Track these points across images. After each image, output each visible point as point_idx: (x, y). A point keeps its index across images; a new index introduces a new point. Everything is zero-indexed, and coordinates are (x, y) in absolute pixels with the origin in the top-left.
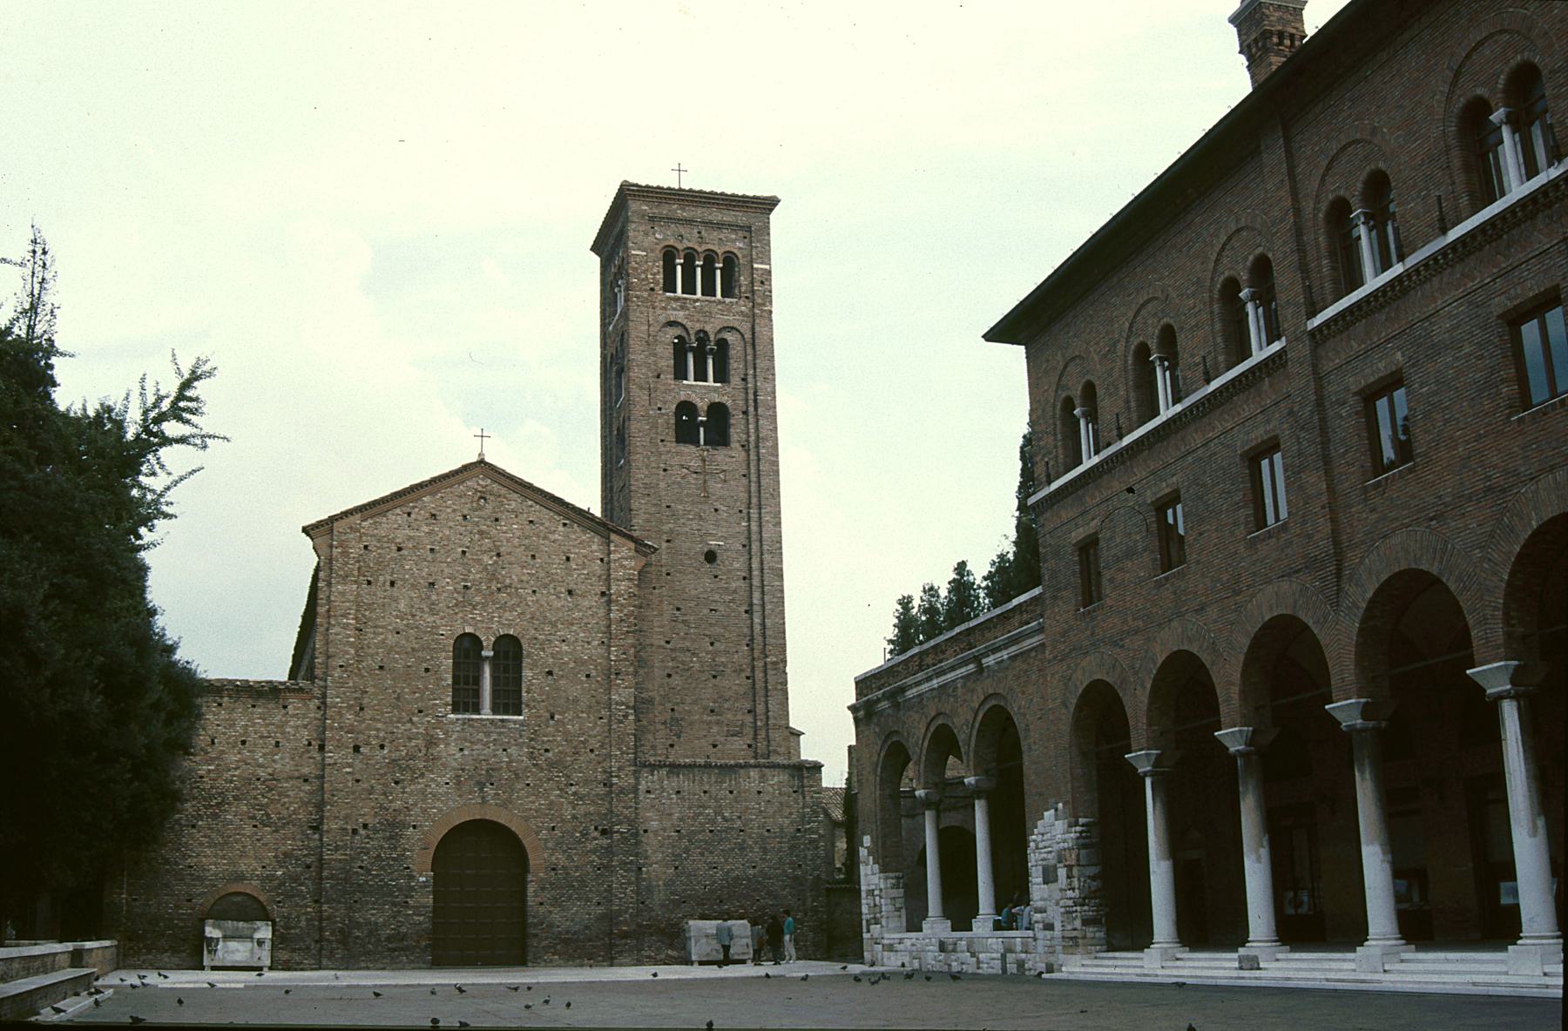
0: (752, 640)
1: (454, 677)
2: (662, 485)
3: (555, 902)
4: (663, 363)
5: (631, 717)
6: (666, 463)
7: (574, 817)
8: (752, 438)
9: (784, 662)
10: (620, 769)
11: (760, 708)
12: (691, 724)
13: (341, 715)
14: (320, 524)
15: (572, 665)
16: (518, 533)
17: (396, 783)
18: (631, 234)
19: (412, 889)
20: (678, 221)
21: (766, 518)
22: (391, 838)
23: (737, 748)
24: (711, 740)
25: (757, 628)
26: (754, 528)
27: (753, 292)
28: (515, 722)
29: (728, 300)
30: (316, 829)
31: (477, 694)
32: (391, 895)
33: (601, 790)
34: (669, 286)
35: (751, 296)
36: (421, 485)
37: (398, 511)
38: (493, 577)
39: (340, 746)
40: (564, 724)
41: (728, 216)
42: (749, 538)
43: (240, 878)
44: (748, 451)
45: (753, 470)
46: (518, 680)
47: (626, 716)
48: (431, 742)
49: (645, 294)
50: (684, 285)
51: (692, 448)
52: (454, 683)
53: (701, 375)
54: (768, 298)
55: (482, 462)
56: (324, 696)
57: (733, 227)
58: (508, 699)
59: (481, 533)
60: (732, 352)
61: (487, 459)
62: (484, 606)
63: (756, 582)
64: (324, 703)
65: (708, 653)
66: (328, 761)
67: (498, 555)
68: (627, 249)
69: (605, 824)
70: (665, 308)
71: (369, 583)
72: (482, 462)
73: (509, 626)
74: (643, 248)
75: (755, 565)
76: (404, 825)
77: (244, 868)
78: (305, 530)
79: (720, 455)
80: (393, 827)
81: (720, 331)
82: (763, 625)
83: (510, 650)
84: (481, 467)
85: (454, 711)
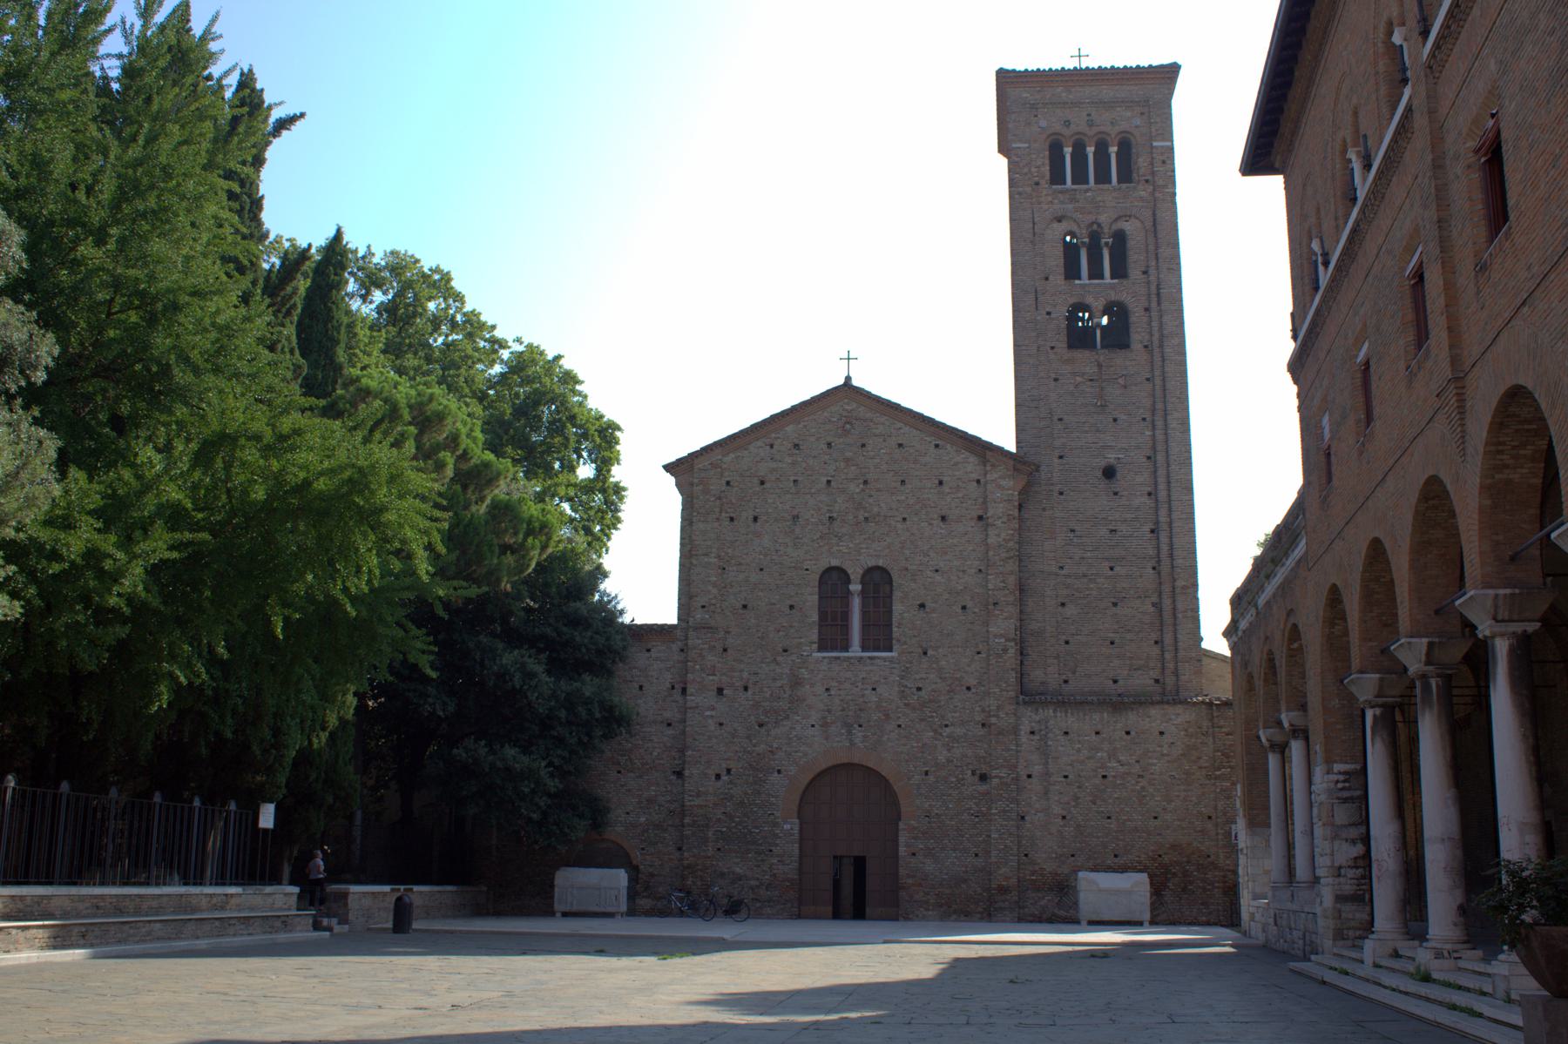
0: (1159, 562)
5: (1012, 651)
7: (949, 761)
9: (1195, 585)
10: (999, 708)
14: (680, 461)
15: (946, 596)
17: (761, 725)
21: (1173, 424)
25: (1165, 548)
27: (1153, 173)
28: (885, 659)
29: (1124, 186)
33: (982, 732)
37: (759, 443)
42: (1154, 448)
44: (1151, 353)
47: (1005, 650)
48: (796, 683)
49: (1028, 189)
51: (1087, 353)
53: (1096, 273)
58: (879, 635)
59: (847, 460)
60: (1131, 244)
61: (855, 383)
63: (1162, 494)
66: (689, 704)
69: (984, 769)
71: (732, 519)
79: (1119, 359)
81: (1116, 220)
83: (879, 582)
85: (820, 649)
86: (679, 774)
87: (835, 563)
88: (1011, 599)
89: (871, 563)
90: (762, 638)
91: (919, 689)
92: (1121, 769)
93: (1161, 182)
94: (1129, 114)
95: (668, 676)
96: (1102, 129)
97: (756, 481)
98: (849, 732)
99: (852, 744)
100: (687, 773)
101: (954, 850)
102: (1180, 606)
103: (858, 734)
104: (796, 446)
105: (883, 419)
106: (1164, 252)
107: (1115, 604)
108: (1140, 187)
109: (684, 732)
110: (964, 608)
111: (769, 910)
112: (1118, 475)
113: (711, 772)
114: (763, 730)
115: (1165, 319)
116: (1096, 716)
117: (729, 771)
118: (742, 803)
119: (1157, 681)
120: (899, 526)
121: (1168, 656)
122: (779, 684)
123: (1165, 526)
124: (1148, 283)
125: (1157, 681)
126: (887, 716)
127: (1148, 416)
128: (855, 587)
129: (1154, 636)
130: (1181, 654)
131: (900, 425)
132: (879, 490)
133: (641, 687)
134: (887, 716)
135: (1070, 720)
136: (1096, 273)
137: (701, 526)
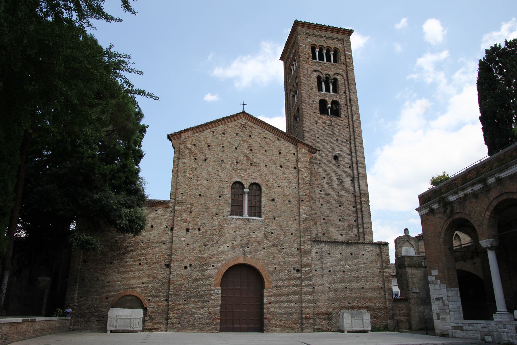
0: (355, 191)
1: (232, 200)
2: (316, 129)
6: (314, 123)
7: (285, 263)
8: (350, 114)
9: (368, 201)
11: (360, 220)
13: (181, 215)
14: (175, 134)
15: (283, 196)
16: (259, 142)
17: (205, 246)
18: (299, 38)
19: (211, 295)
20: (316, 36)
21: (357, 143)
22: (202, 271)
23: (351, 236)
25: (357, 187)
27: (346, 62)
28: (258, 220)
30: (168, 266)
31: (241, 206)
32: (201, 297)
34: (314, 57)
36: (219, 120)
37: (208, 131)
38: (248, 159)
39: (180, 228)
41: (336, 35)
43: (132, 288)
44: (348, 118)
45: (351, 126)
46: (260, 201)
47: (306, 219)
48: (221, 228)
50: (318, 60)
52: (232, 203)
53: (328, 90)
54: (352, 64)
55: (244, 112)
56: (174, 206)
57: (337, 39)
58: (256, 210)
59: (244, 141)
60: (339, 83)
63: (355, 168)
64: (174, 209)
65: (337, 196)
67: (251, 150)
68: (298, 44)
71: (196, 159)
72: (244, 112)
75: (354, 162)
76: (209, 266)
77: (133, 283)
78: (170, 137)
79: (337, 120)
80: (204, 264)
82: (359, 186)
85: (232, 215)
86: (168, 266)
87: (238, 180)
88: (308, 199)
89: (253, 181)
90: (207, 209)
91: (272, 233)
92: (350, 268)
95: (165, 222)
96: (328, 45)
97: (206, 145)
98: (244, 250)
99: (245, 255)
100: (172, 265)
101: (287, 301)
102: (364, 208)
103: (247, 251)
104: (223, 133)
106: (351, 87)
107: (340, 206)
109: (171, 247)
110: (289, 201)
111: (207, 329)
112: (340, 159)
113: (183, 265)
114: (206, 248)
115: (353, 108)
116: (340, 247)
117: (191, 265)
118: (196, 279)
119: (356, 235)
121: (360, 226)
122: (214, 228)
123: (356, 179)
124: (346, 96)
125: (356, 235)
126: (259, 244)
127: (349, 141)
128: (246, 190)
129: (355, 219)
130: (365, 225)
131: (264, 130)
132: (256, 153)
133: (152, 227)
134: (259, 244)
135: (331, 248)
136: (328, 90)
137: (183, 160)
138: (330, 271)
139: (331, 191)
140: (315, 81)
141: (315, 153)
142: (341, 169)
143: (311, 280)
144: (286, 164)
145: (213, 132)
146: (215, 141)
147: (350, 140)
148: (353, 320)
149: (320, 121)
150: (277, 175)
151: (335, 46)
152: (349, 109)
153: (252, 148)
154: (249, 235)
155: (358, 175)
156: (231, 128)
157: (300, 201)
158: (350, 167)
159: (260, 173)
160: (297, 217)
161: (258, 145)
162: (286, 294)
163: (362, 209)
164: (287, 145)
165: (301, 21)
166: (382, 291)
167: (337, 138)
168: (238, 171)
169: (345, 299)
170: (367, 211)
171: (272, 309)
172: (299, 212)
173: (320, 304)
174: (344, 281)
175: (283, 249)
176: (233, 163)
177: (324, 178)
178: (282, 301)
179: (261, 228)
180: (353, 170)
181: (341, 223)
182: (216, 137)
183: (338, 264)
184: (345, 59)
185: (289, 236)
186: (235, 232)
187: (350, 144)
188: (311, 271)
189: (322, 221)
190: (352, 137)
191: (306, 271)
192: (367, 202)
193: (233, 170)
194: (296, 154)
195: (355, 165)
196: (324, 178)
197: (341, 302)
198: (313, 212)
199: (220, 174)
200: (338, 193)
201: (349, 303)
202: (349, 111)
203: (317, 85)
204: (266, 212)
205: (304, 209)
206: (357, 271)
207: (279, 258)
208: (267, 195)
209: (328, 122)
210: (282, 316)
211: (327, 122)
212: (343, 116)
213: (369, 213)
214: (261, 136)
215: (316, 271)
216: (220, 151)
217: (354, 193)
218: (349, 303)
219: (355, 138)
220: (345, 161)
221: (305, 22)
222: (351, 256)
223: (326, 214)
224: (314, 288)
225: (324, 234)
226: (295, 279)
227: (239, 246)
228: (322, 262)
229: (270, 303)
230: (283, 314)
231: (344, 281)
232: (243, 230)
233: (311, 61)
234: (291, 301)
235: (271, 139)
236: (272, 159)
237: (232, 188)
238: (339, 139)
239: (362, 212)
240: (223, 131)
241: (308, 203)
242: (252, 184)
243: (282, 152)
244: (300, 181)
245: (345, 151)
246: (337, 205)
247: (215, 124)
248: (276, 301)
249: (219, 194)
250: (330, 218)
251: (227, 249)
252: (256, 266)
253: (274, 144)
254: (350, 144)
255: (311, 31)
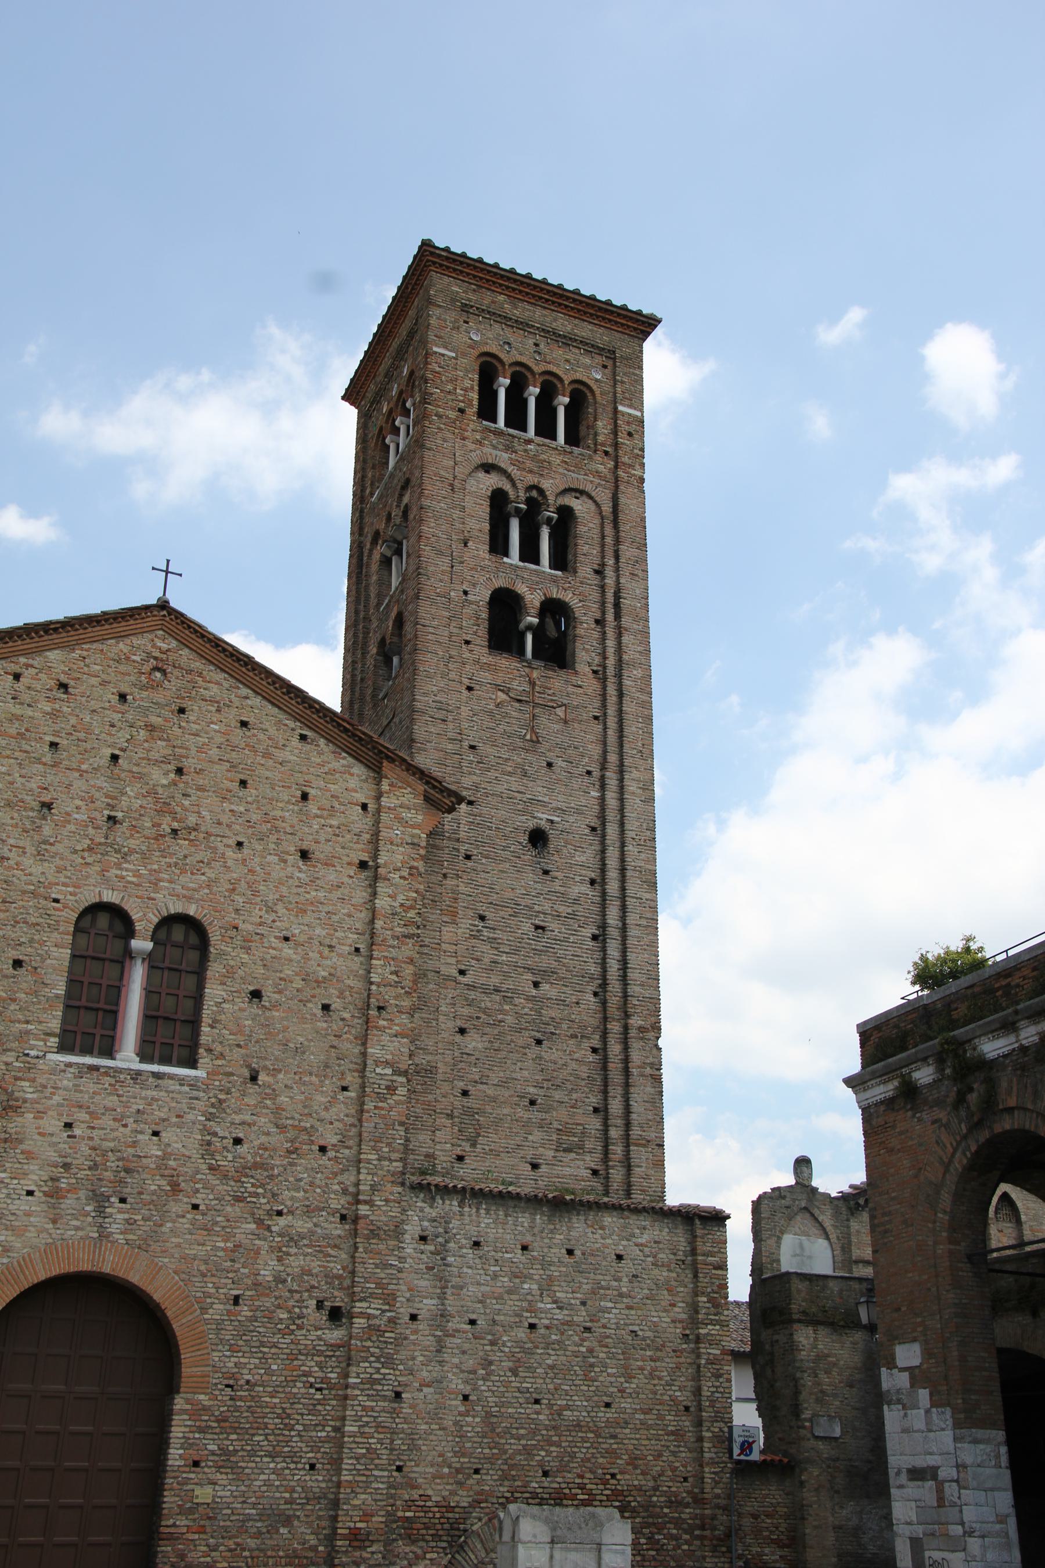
0: (604, 984)
1: (73, 982)
2: (465, 712)
3: (226, 1460)
4: (472, 524)
5: (402, 1091)
7: (279, 1280)
8: (611, 662)
9: (657, 1028)
10: (374, 1188)
11: (616, 1106)
12: (498, 1121)
15: (298, 984)
16: (219, 739)
18: (433, 321)
20: (505, 320)
21: (631, 786)
23: (573, 1172)
24: (529, 1154)
25: (614, 966)
26: (612, 801)
27: (616, 445)
28: (181, 1081)
31: (112, 1015)
33: (339, 1230)
34: (487, 411)
35: (614, 453)
36: (47, 628)
38: (164, 808)
40: (274, 1095)
41: (585, 330)
44: (604, 681)
45: (611, 711)
46: (198, 998)
47: (391, 1089)
52: (69, 994)
53: (530, 554)
54: (639, 455)
55: (163, 605)
57: (591, 348)
58: (174, 1036)
59: (151, 728)
60: (581, 529)
62: (145, 857)
63: (613, 887)
65: (530, 999)
67: (180, 771)
68: (424, 342)
69: (339, 1299)
70: (480, 443)
72: (163, 605)
73: (189, 899)
74: (454, 347)
75: (612, 862)
79: (557, 682)
82: (624, 962)
84: (163, 614)
85: (64, 1048)
87: (109, 896)
88: (406, 1003)
91: (238, 1141)
92: (560, 1315)
93: (625, 459)
94: (588, 361)
96: (555, 370)
98: (100, 1211)
99: (104, 1236)
101: (273, 1456)
102: (636, 1056)
104: (63, 686)
105: (220, 676)
106: (627, 552)
107: (539, 1042)
108: (598, 457)
110: (326, 1008)
115: (625, 639)
116: (524, 1219)
119: (595, 1172)
120: (229, 853)
121: (614, 1133)
123: (613, 932)
124: (603, 588)
125: (595, 1172)
126: (175, 1188)
127: (596, 774)
128: (141, 944)
130: (635, 1132)
131: (244, 691)
132: (201, 789)
134: (175, 1188)
135: (484, 1222)
136: (530, 554)
138: (472, 1322)
139: (506, 975)
140: (483, 510)
141: (451, 810)
142: (557, 886)
143: (389, 1361)
144: (328, 848)
145: (17, 677)
146: (19, 718)
147: (603, 768)
148: (557, 1555)
149: (486, 676)
150: (284, 890)
151: (578, 376)
152: (611, 643)
153: (188, 764)
154: (134, 1144)
155: (623, 918)
156: (97, 665)
157: (370, 1010)
158: (593, 882)
159: (211, 874)
160: (351, 1079)
161: (214, 752)
162: (272, 1422)
163: (626, 1061)
164: (336, 765)
165: (447, 249)
166: (687, 1423)
167: (551, 756)
168: (114, 858)
169: (528, 1451)
170: (648, 1071)
171: (204, 1494)
172: (364, 1054)
173: (420, 1471)
174: (531, 1369)
175: (280, 1213)
176: (92, 820)
177: (482, 918)
178: (252, 1453)
179: (190, 1117)
180: (604, 894)
181: (535, 1115)
182: (26, 697)
183: (510, 1292)
184: (615, 432)
185: (311, 1159)
186: (68, 1126)
187: (603, 787)
188: (392, 1321)
189: (459, 1102)
190: (613, 758)
191: (369, 1317)
192: (651, 1035)
193: (90, 849)
194: (371, 807)
195: (613, 874)
196: (482, 918)
197: (512, 1467)
198: (421, 1059)
199: (27, 862)
200: (536, 985)
201: (545, 1474)
202: (611, 651)
203: (487, 526)
204: (219, 1048)
205: (386, 1046)
206: (587, 1329)
207: (258, 1252)
208: (230, 972)
209: (519, 686)
210: (242, 1530)
211: (515, 685)
212: (582, 668)
213: (657, 1080)
214: (232, 716)
215: (414, 1317)
216: (39, 761)
217: (601, 992)
218: (545, 1474)
219: (621, 764)
220: (575, 855)
221: (464, 255)
222: (567, 1259)
223: (475, 1073)
224: (398, 1395)
225: (460, 1158)
226: (320, 1353)
227: (82, 1194)
228: (443, 1282)
229: (196, 1464)
230: (249, 1518)
231: (531, 1369)
232: (107, 1121)
233: (473, 423)
234: (293, 1456)
235: (272, 731)
236: (266, 818)
237: (78, 929)
238: (559, 763)
239: (626, 1072)
240: (64, 679)
241: (404, 1019)
242: (170, 921)
243: (312, 792)
244: (379, 924)
245: (579, 812)
246: (525, 1038)
247: (27, 644)
248: (224, 1451)
249: (14, 954)
250: (490, 1092)
251: (24, 1204)
252: (149, 1289)
253: (280, 755)
254: (603, 787)
255: (487, 299)
